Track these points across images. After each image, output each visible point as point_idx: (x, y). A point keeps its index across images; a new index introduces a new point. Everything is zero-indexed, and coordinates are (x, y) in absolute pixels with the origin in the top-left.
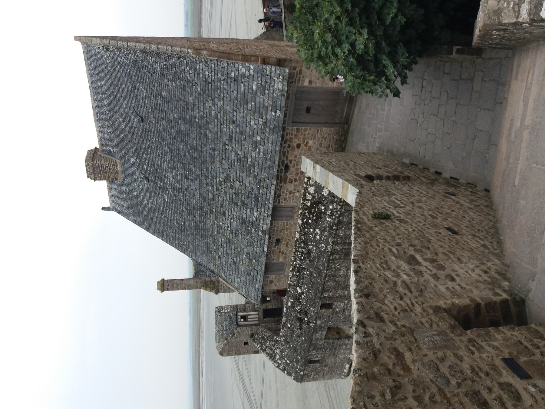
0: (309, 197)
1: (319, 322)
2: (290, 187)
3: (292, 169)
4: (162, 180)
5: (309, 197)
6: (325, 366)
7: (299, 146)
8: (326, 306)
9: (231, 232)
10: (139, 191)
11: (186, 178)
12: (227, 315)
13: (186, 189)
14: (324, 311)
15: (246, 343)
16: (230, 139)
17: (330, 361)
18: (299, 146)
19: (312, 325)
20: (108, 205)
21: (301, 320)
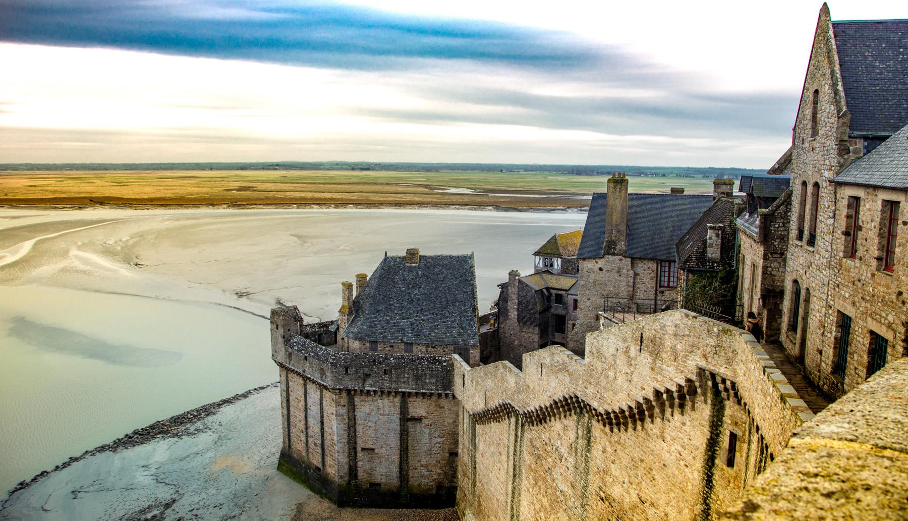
0: (440, 358)
1: (376, 370)
2: (424, 349)
3: (433, 350)
4: (413, 287)
5: (440, 358)
6: (343, 377)
7: (444, 351)
8: (385, 372)
9: (394, 323)
10: (403, 274)
11: (418, 300)
12: (295, 314)
13: (412, 300)
14: (383, 371)
15: (289, 330)
16: (443, 322)
17: (347, 378)
18: (444, 351)
19: (374, 367)
20: (388, 255)
21: (374, 361)
